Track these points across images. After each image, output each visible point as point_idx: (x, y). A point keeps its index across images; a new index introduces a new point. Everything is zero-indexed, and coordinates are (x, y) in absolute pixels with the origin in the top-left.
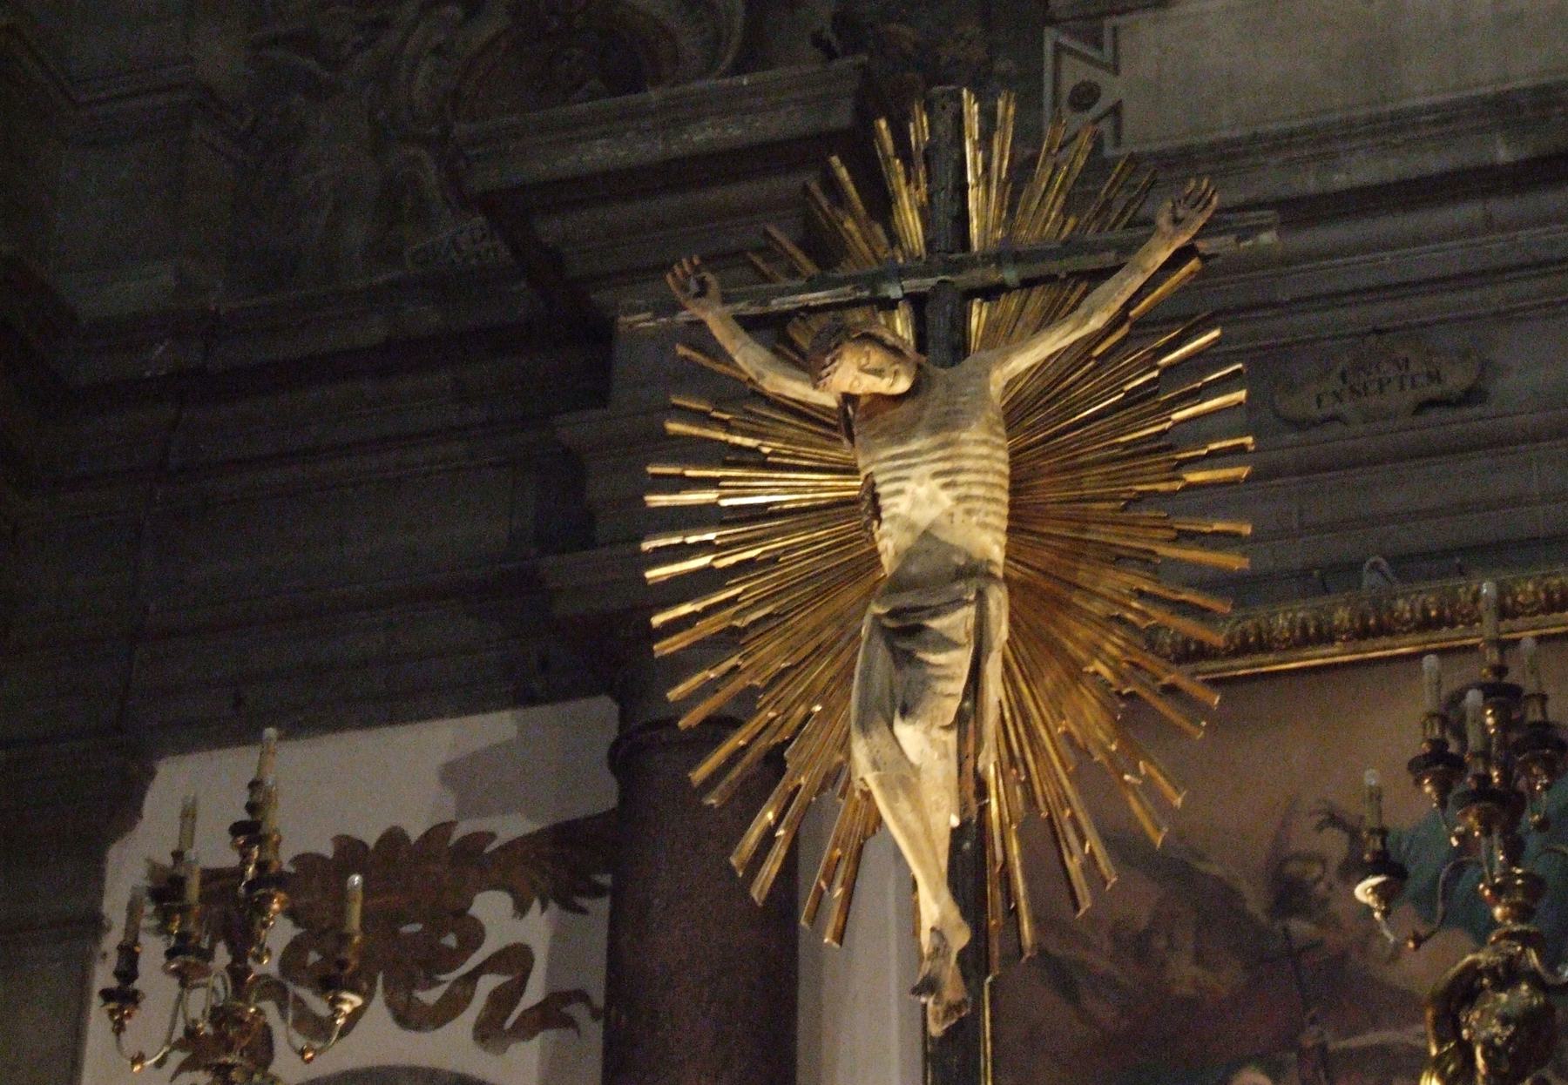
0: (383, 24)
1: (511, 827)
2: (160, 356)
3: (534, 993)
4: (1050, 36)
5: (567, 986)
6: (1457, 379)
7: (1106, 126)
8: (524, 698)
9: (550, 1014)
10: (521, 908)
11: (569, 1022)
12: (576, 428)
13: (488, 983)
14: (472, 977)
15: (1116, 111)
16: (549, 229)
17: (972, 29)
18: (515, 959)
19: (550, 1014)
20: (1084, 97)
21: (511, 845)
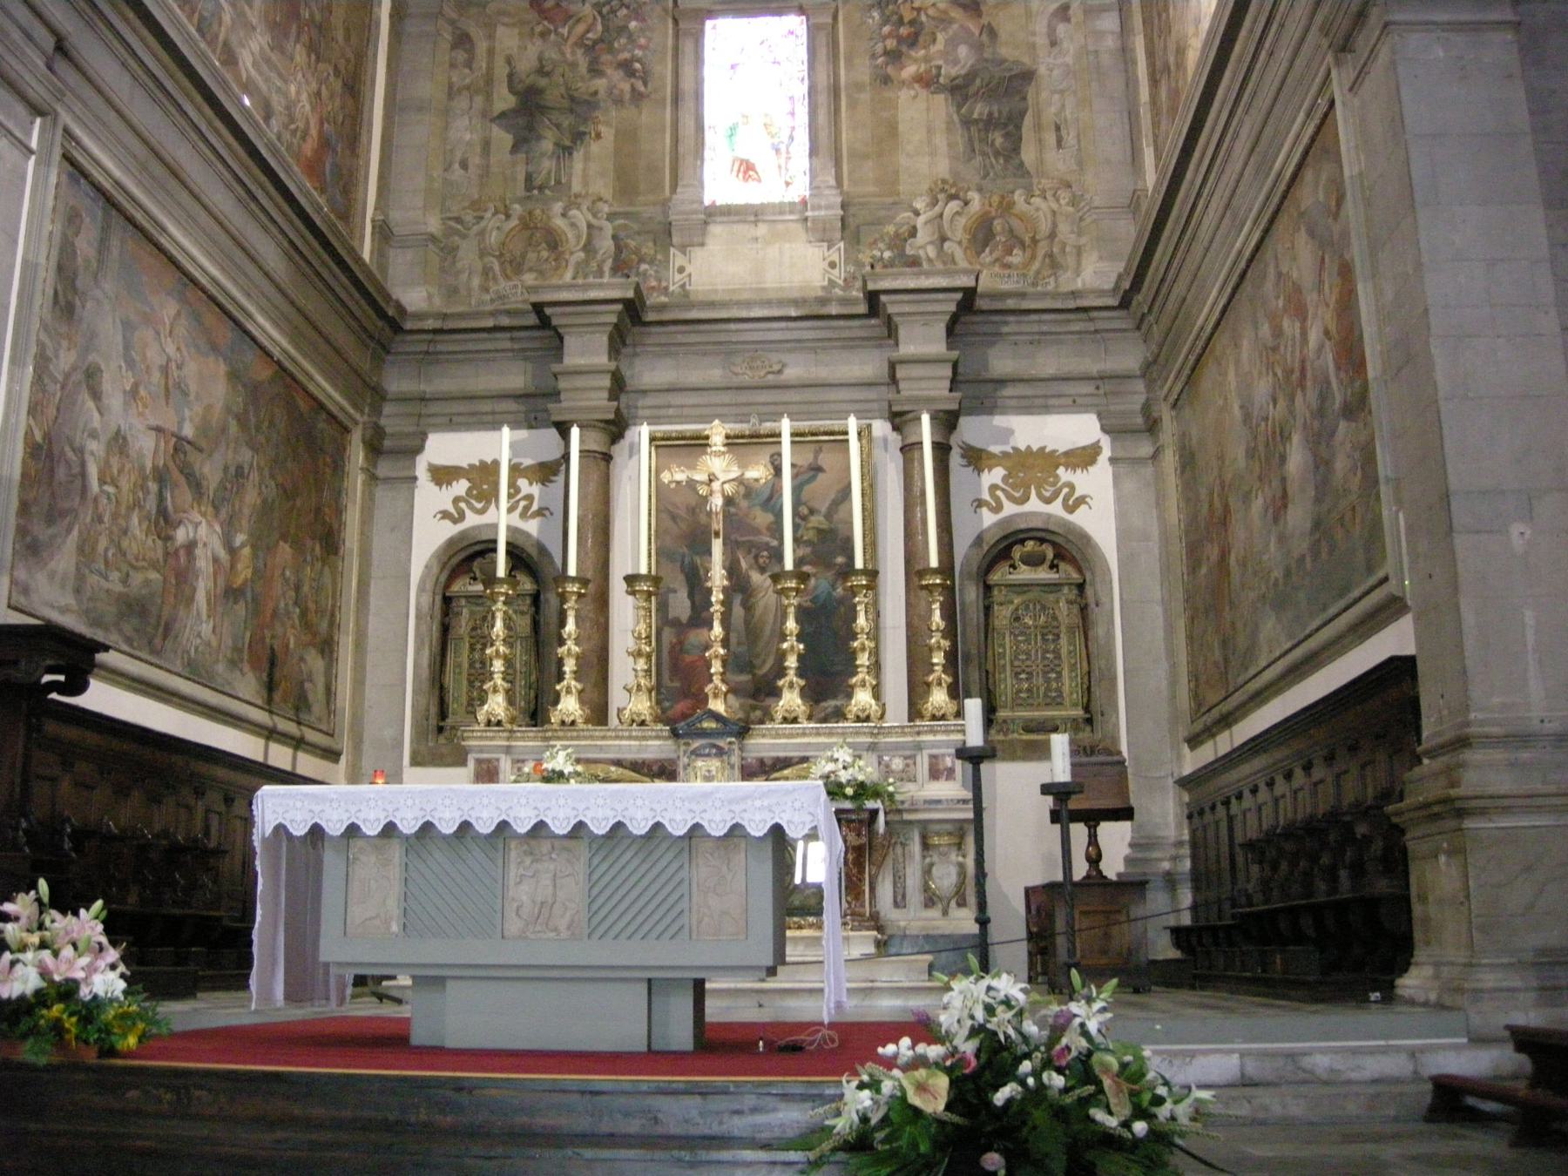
0: (482, 218)
1: (527, 462)
2: (430, 324)
3: (535, 507)
4: (672, 250)
5: (543, 505)
6: (776, 368)
7: (687, 280)
8: (531, 427)
9: (540, 512)
10: (531, 484)
11: (544, 515)
12: (556, 368)
13: (522, 503)
14: (518, 501)
15: (690, 275)
16: (548, 311)
17: (650, 244)
18: (530, 498)
19: (540, 512)
20: (681, 270)
21: (527, 467)
